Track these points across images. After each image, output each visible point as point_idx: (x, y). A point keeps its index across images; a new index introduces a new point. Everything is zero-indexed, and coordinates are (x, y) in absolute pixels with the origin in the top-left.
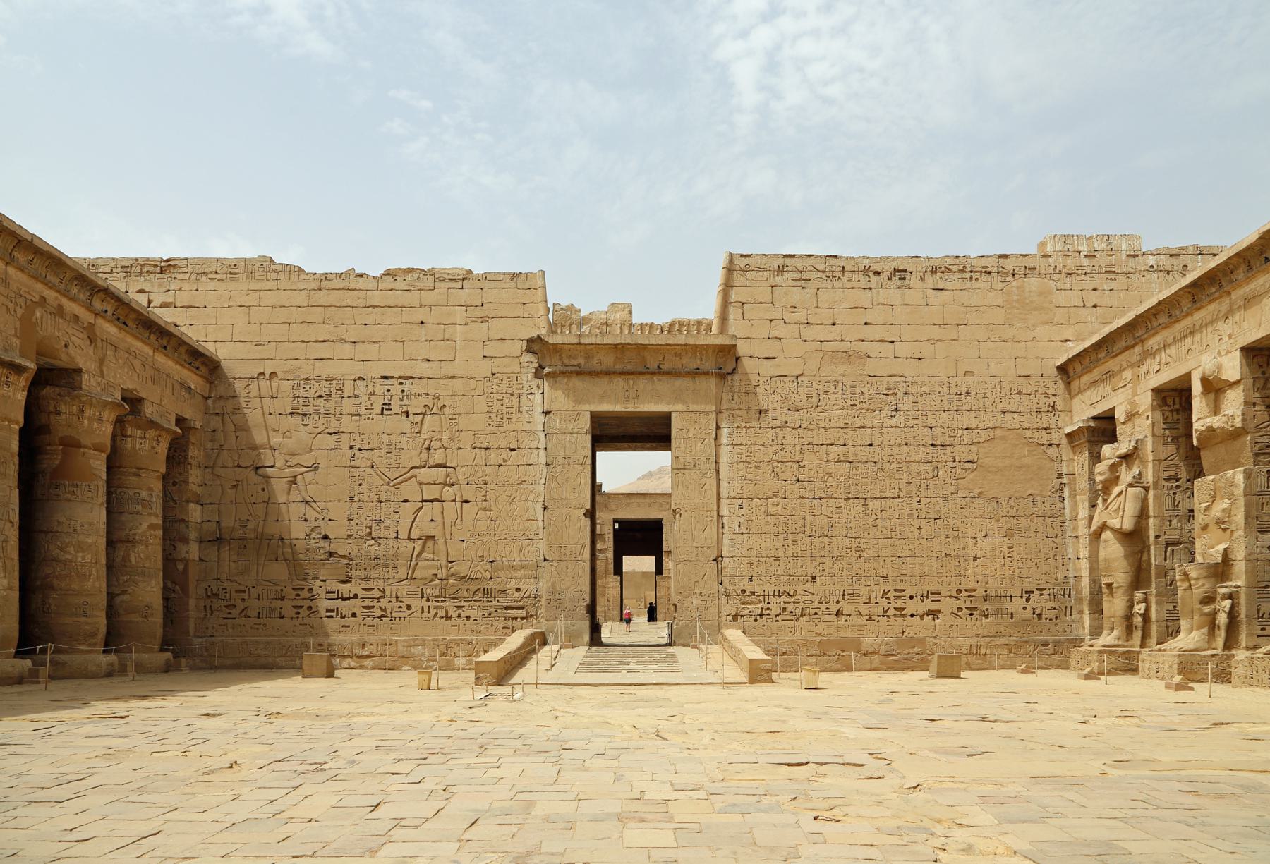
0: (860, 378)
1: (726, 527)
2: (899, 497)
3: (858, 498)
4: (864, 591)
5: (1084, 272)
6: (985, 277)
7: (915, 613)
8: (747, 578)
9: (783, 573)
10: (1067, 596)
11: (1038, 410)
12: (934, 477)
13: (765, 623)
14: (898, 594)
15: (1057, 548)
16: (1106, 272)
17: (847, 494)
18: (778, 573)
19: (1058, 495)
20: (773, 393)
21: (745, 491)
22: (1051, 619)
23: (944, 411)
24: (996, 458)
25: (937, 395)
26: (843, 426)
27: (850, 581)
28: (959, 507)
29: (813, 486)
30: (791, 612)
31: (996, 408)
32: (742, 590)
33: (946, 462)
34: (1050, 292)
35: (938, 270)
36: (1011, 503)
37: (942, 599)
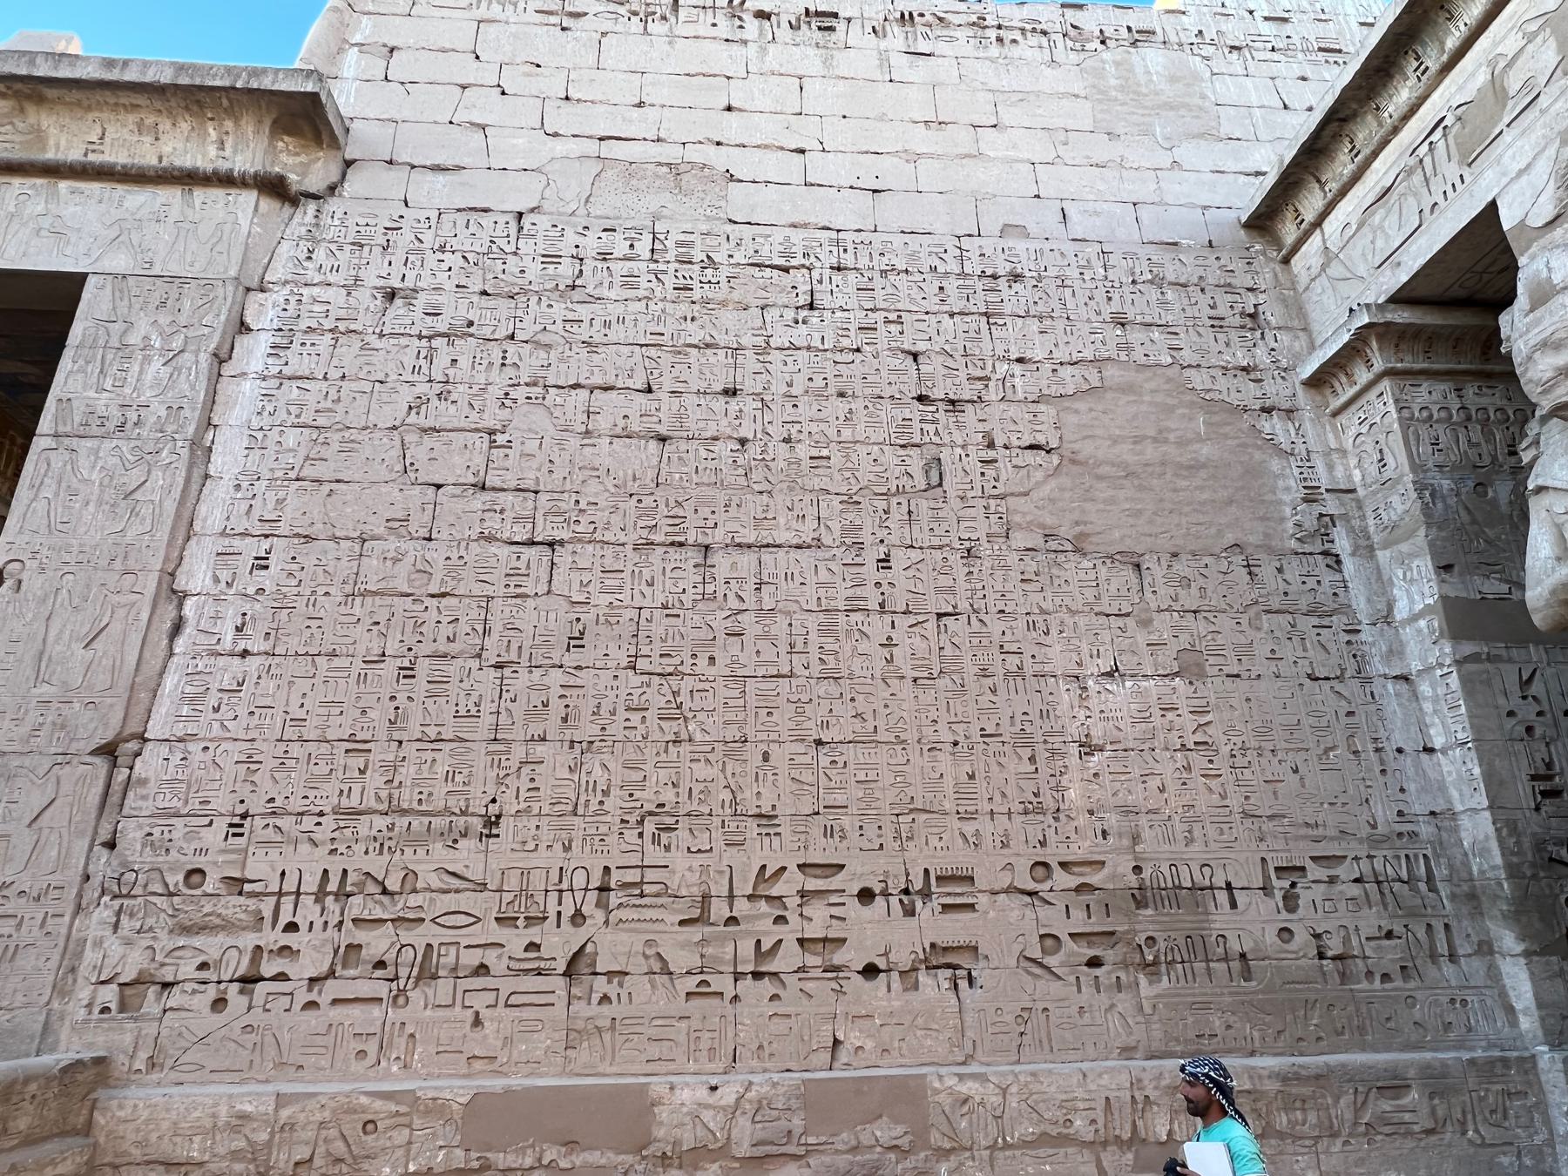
0: (704, 228)
1: (188, 630)
2: (818, 544)
3: (681, 545)
4: (683, 871)
5: (1269, 46)
6: (1034, 40)
7: (882, 964)
8: (221, 825)
9: (373, 804)
10: (1423, 886)
11: (1216, 323)
12: (929, 487)
13: (256, 1018)
14: (813, 884)
15: (1350, 714)
16: (1320, 49)
17: (644, 533)
18: (354, 802)
19: (1318, 548)
20: (442, 249)
21: (289, 513)
22: (1386, 977)
23: (952, 315)
24: (1115, 441)
25: (928, 277)
26: (650, 339)
27: (631, 836)
28: (1015, 576)
29: (530, 504)
30: (381, 964)
31: (1098, 313)
32: (190, 873)
33: (963, 447)
34: (1196, 77)
35: (917, 19)
36: (1181, 568)
37: (982, 900)
